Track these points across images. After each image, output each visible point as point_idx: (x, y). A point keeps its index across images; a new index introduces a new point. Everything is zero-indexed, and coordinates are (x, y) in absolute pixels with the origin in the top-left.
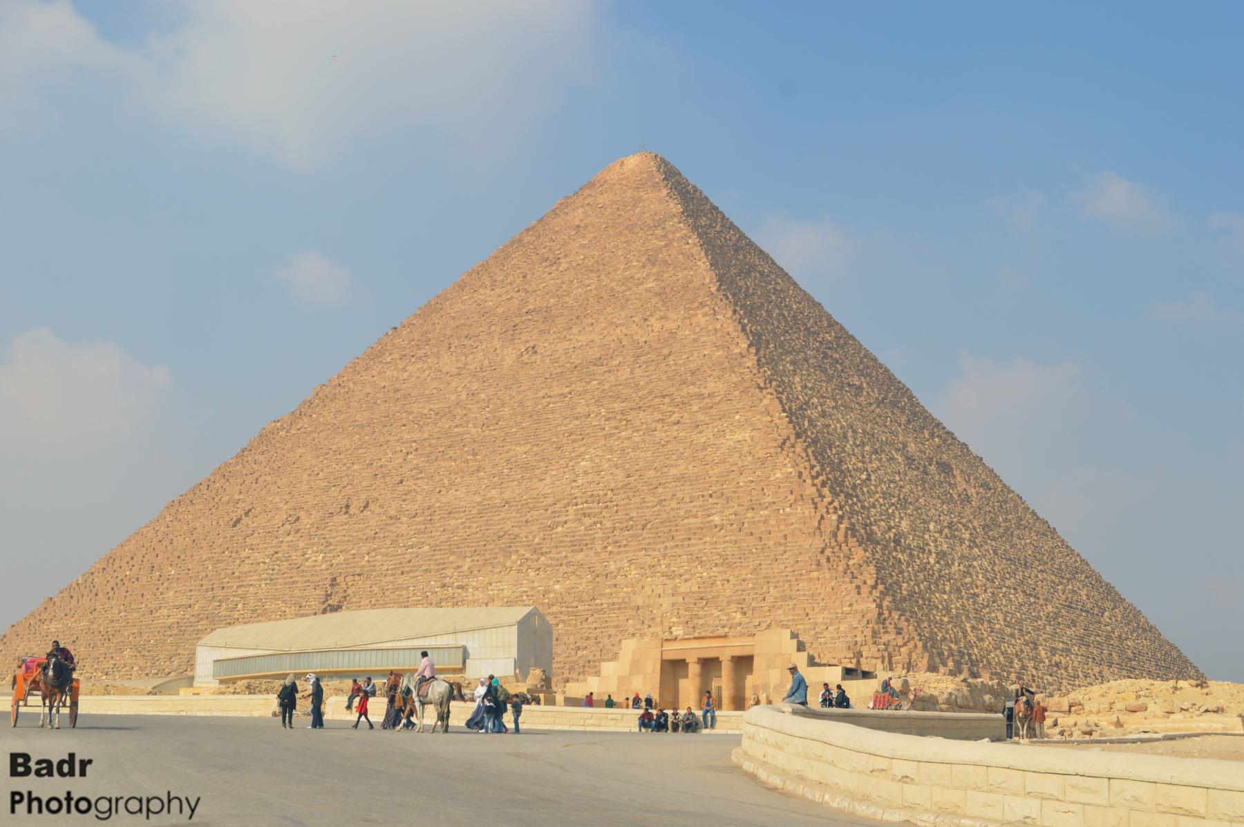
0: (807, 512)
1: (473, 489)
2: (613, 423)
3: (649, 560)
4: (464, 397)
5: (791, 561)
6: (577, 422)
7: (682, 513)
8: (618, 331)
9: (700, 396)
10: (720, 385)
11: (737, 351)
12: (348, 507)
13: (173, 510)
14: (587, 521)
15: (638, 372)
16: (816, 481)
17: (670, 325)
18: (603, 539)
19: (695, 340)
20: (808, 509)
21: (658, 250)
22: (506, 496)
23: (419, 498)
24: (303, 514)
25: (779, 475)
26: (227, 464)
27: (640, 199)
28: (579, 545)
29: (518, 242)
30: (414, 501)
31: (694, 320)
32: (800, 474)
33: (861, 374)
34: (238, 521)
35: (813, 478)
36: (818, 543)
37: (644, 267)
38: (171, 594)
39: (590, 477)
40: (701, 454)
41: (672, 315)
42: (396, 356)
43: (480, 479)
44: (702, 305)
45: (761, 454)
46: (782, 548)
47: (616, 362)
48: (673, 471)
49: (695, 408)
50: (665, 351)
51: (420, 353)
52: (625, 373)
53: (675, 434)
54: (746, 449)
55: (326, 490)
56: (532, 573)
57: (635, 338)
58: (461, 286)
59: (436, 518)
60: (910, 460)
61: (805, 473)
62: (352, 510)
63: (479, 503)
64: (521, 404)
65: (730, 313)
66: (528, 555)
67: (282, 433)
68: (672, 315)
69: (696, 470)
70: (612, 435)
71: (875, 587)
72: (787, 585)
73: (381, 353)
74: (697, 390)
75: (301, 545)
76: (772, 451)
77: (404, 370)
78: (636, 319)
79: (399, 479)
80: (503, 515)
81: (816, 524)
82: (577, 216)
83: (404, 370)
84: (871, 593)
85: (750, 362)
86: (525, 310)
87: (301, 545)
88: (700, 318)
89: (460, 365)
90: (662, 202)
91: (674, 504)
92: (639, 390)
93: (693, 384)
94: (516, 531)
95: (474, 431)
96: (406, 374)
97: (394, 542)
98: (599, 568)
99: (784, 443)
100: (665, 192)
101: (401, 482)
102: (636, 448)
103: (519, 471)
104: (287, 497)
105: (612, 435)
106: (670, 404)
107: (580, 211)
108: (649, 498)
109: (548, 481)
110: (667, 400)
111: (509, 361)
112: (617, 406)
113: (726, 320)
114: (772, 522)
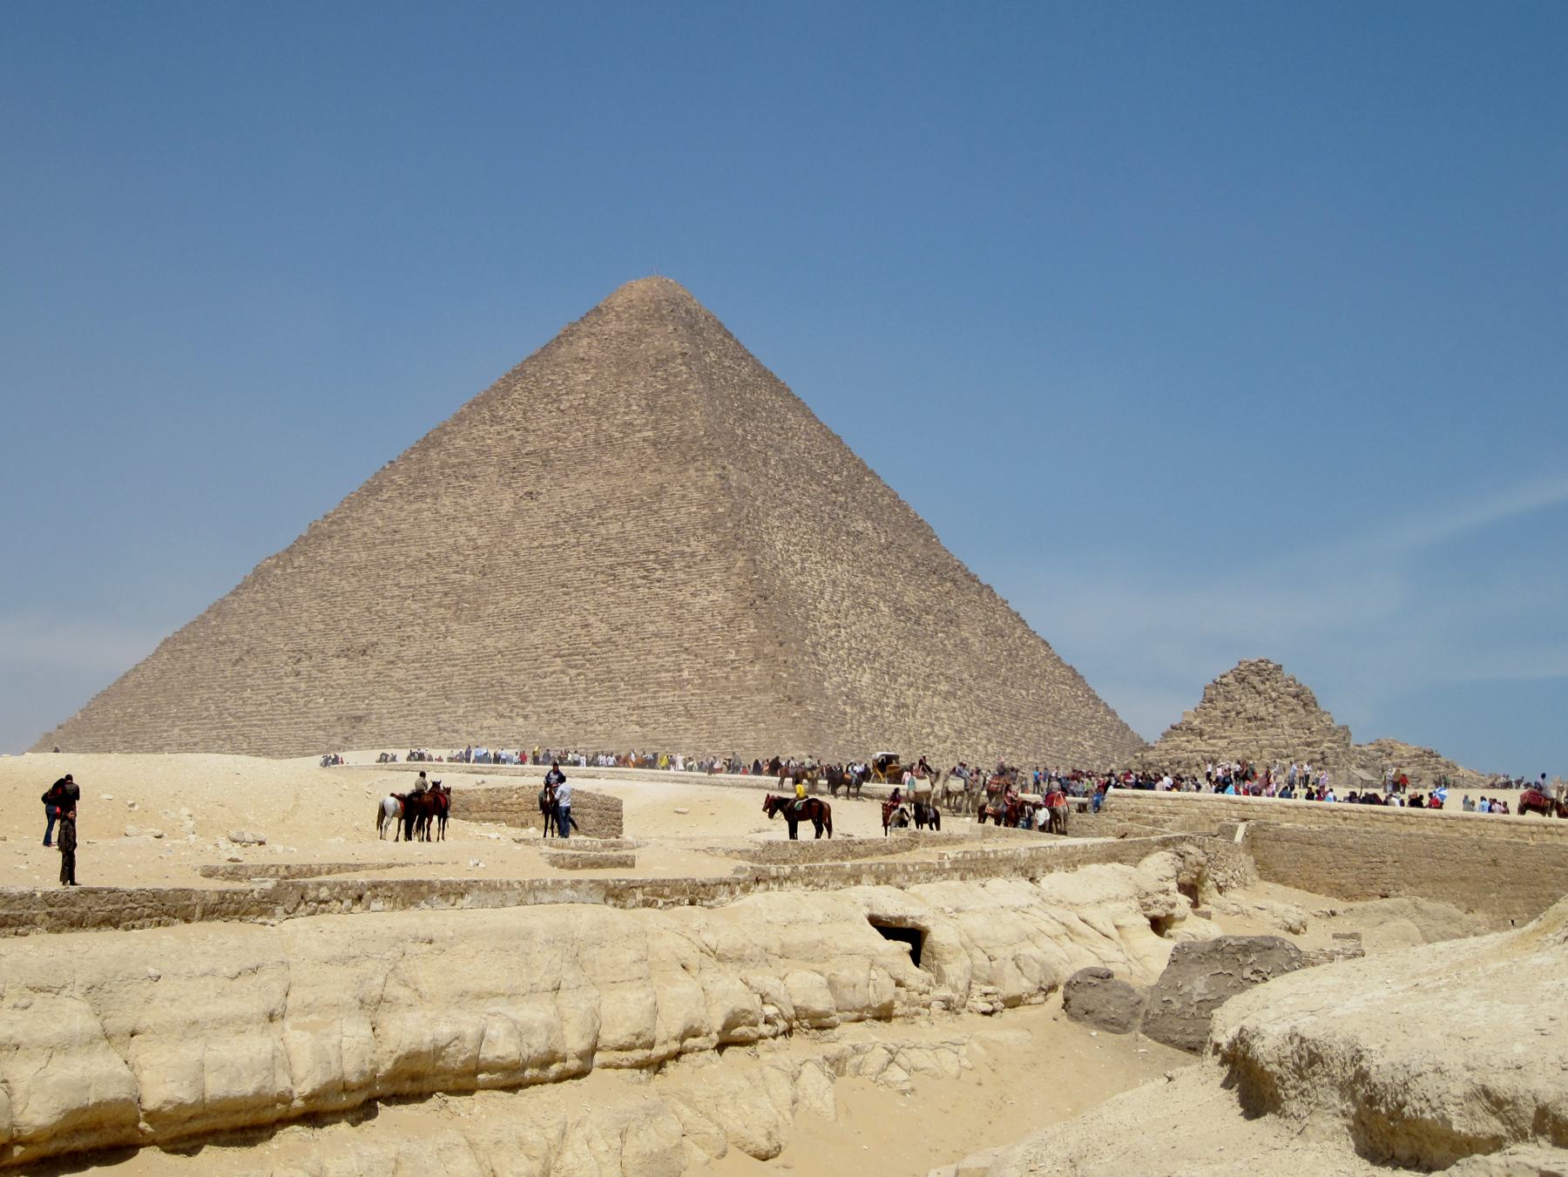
2: (600, 577)
3: (623, 711)
9: (682, 554)
10: (702, 544)
13: (170, 647)
14: (573, 672)
15: (629, 526)
18: (586, 690)
19: (683, 497)
21: (656, 395)
22: (501, 644)
26: (223, 601)
29: (518, 373)
33: (868, 516)
38: (176, 731)
40: (678, 612)
41: (665, 468)
42: (395, 494)
44: (694, 459)
48: (652, 628)
50: (655, 507)
52: (614, 528)
56: (520, 721)
58: (460, 419)
60: (900, 610)
64: (516, 554)
67: (278, 572)
68: (665, 468)
73: (380, 488)
75: (303, 686)
82: (582, 346)
90: (666, 339)
91: (651, 659)
94: (509, 679)
98: (578, 715)
106: (655, 561)
107: (585, 342)
108: (627, 652)
110: (652, 557)
111: (506, 506)
112: (608, 561)
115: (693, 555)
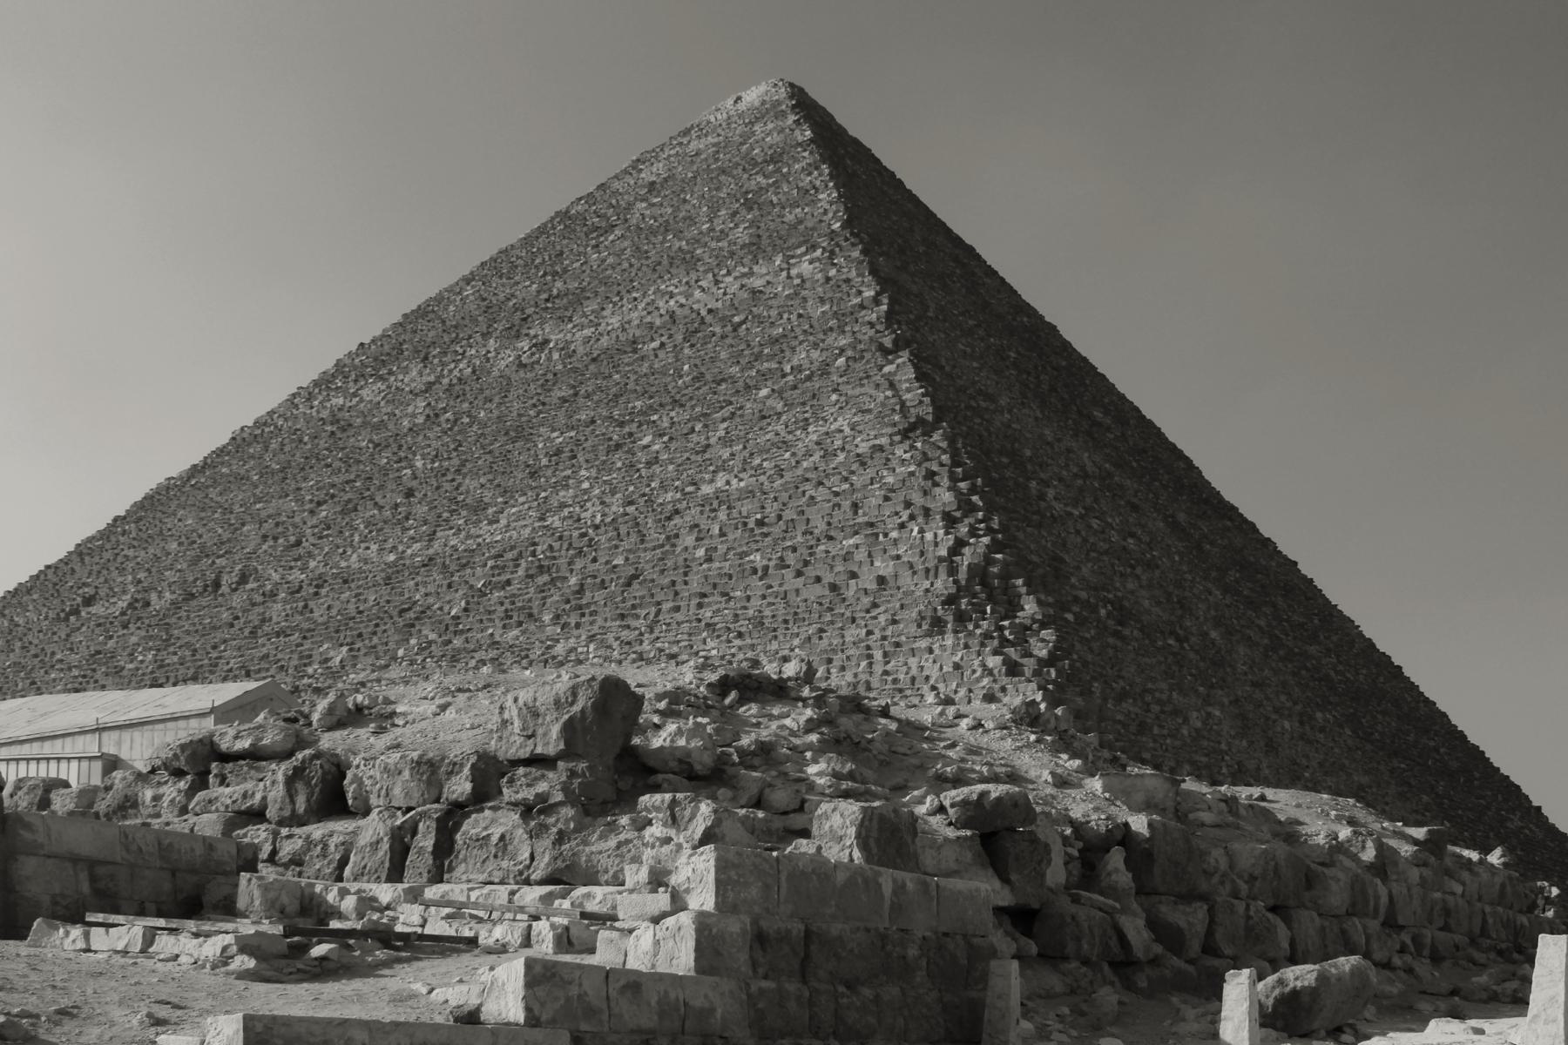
0: (929, 536)
1: (389, 545)
4: (420, 420)
5: (882, 619)
6: (573, 434)
7: (701, 553)
8: (672, 303)
10: (815, 354)
11: (857, 301)
12: (217, 584)
16: (963, 485)
17: (758, 283)
20: (937, 528)
21: (761, 190)
23: (312, 564)
24: (153, 596)
25: (890, 480)
30: (303, 569)
31: (794, 272)
32: (930, 475)
35: (954, 479)
36: (943, 585)
37: (735, 214)
39: (566, 512)
43: (405, 529)
45: (863, 448)
46: (866, 601)
47: (655, 344)
48: (707, 489)
49: (764, 392)
50: (736, 319)
51: (383, 371)
53: (722, 433)
54: (838, 443)
55: (195, 561)
57: (695, 307)
59: (323, 591)
61: (944, 472)
65: (856, 254)
66: (432, 636)
69: (742, 484)
70: (618, 446)
71: (1051, 661)
72: (864, 664)
74: (774, 366)
76: (884, 441)
77: (355, 395)
78: (703, 283)
79: (293, 539)
80: (419, 579)
81: (944, 552)
83: (355, 395)
84: (1037, 673)
86: (545, 296)
87: (134, 639)
89: (432, 378)
92: (681, 377)
93: (771, 357)
95: (419, 464)
96: (355, 400)
101: (298, 543)
103: (464, 513)
104: (141, 575)
105: (618, 446)
109: (503, 522)
113: (850, 264)
114: (861, 555)
115: (797, 369)
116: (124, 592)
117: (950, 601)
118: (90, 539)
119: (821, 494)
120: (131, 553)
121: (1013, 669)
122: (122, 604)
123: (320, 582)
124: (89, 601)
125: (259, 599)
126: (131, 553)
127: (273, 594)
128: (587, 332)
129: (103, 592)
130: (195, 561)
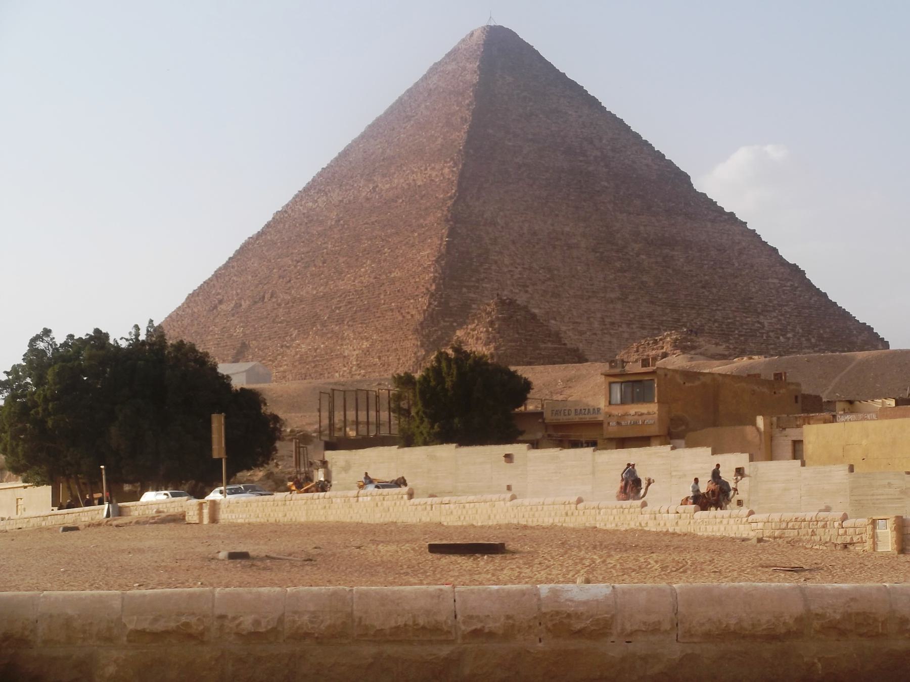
12: (264, 297)
24: (243, 303)
27: (464, 69)
28: (340, 321)
30: (290, 294)
34: (215, 307)
55: (257, 286)
62: (266, 300)
63: (314, 295)
68: (437, 167)
85: (450, 203)
88: (446, 170)
97: (274, 322)
99: (439, 257)
100: (478, 64)
102: (385, 260)
104: (239, 291)
116: (233, 299)
117: (421, 324)
118: (220, 269)
119: (412, 281)
120: (235, 278)
121: (422, 346)
122: (232, 305)
123: (294, 300)
124: (221, 302)
125: (276, 306)
126: (235, 278)
127: (279, 305)
128: (387, 186)
129: (225, 298)
130: (257, 286)
